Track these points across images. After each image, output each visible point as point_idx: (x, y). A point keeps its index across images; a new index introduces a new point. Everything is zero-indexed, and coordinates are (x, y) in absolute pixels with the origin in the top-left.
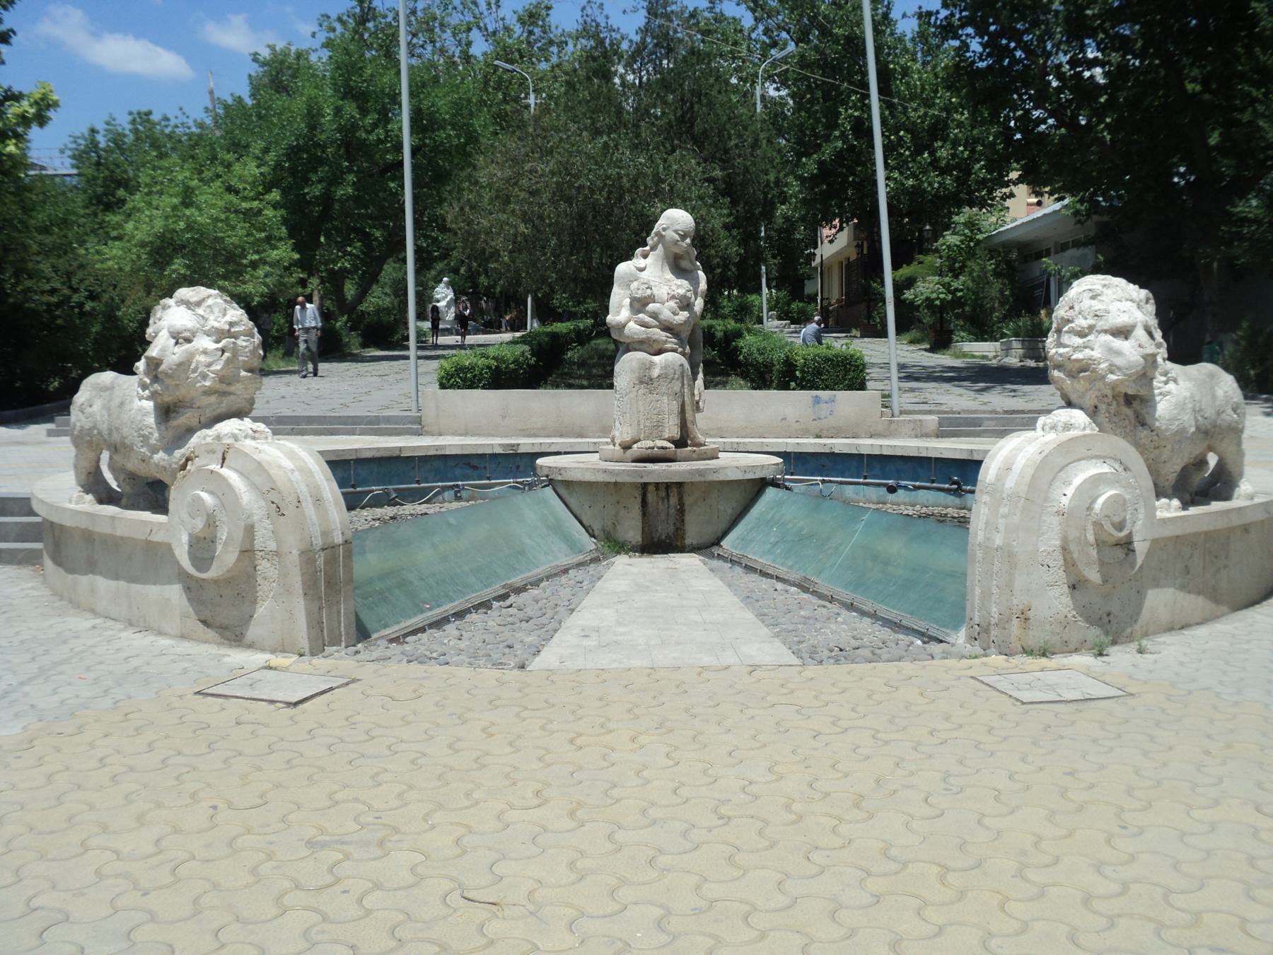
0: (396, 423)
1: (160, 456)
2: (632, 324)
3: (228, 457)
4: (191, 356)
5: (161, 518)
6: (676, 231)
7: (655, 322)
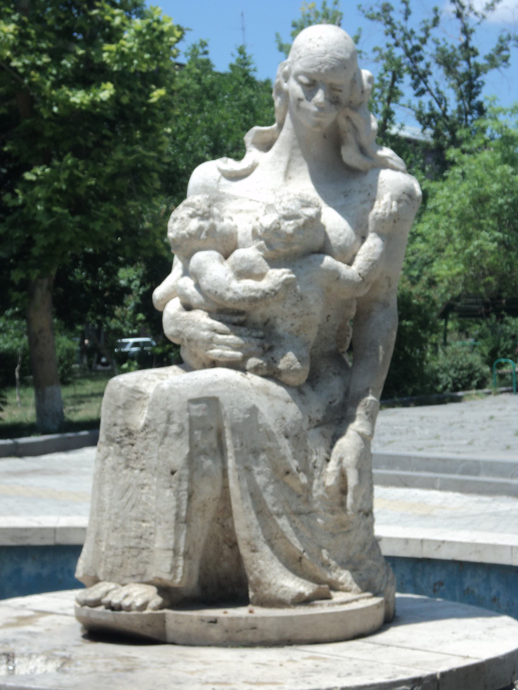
0: (502, 474)
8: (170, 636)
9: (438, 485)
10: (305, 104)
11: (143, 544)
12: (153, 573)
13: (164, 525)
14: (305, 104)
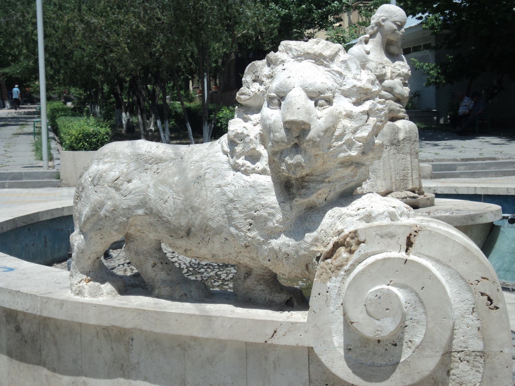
0: (36, 178)
1: (283, 241)
3: (417, 242)
4: (336, 119)
5: (298, 316)
6: (394, 22)
7: (390, 95)
8: (420, 206)
9: (7, 186)
10: (397, 32)
11: (405, 178)
12: (410, 187)
13: (416, 171)
14: (397, 32)
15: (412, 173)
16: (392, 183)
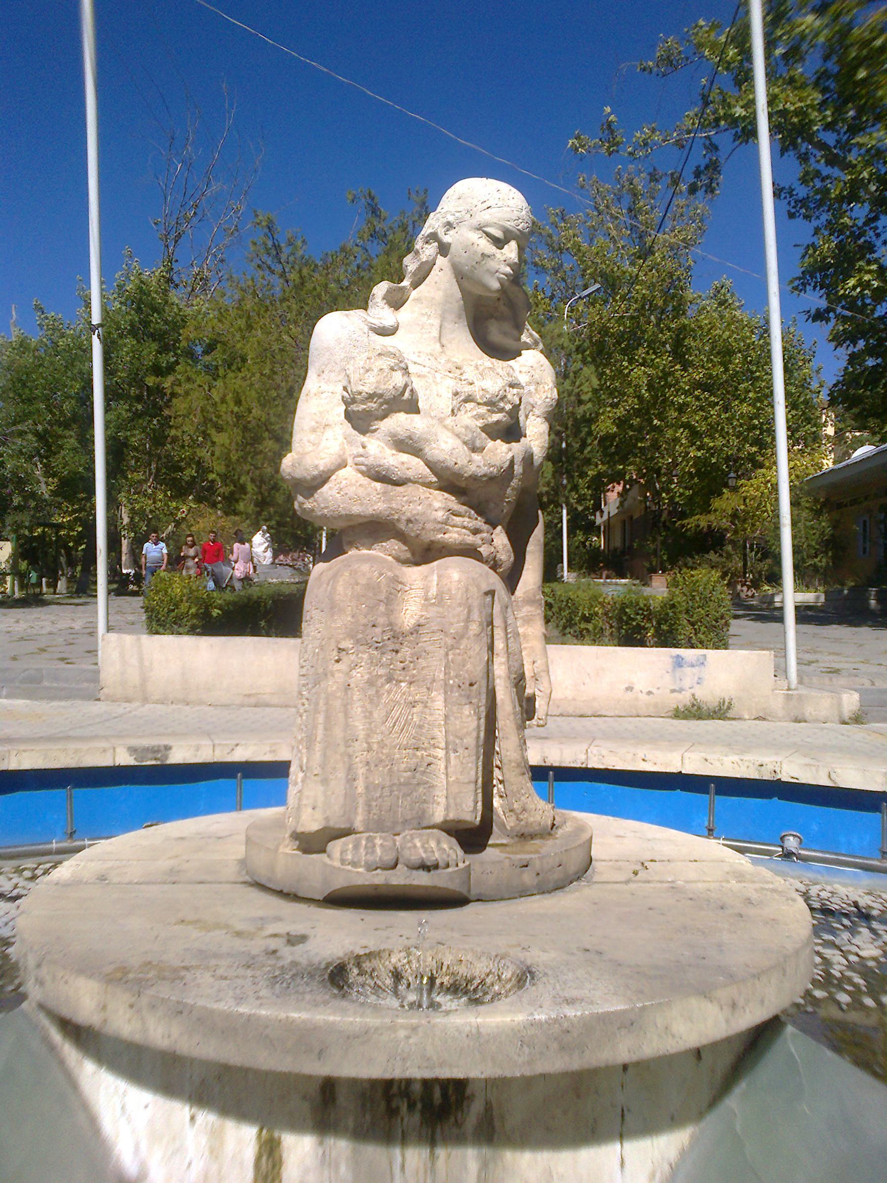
2: (348, 474)
12: (439, 815)
15: (448, 760)
16: (350, 796)
